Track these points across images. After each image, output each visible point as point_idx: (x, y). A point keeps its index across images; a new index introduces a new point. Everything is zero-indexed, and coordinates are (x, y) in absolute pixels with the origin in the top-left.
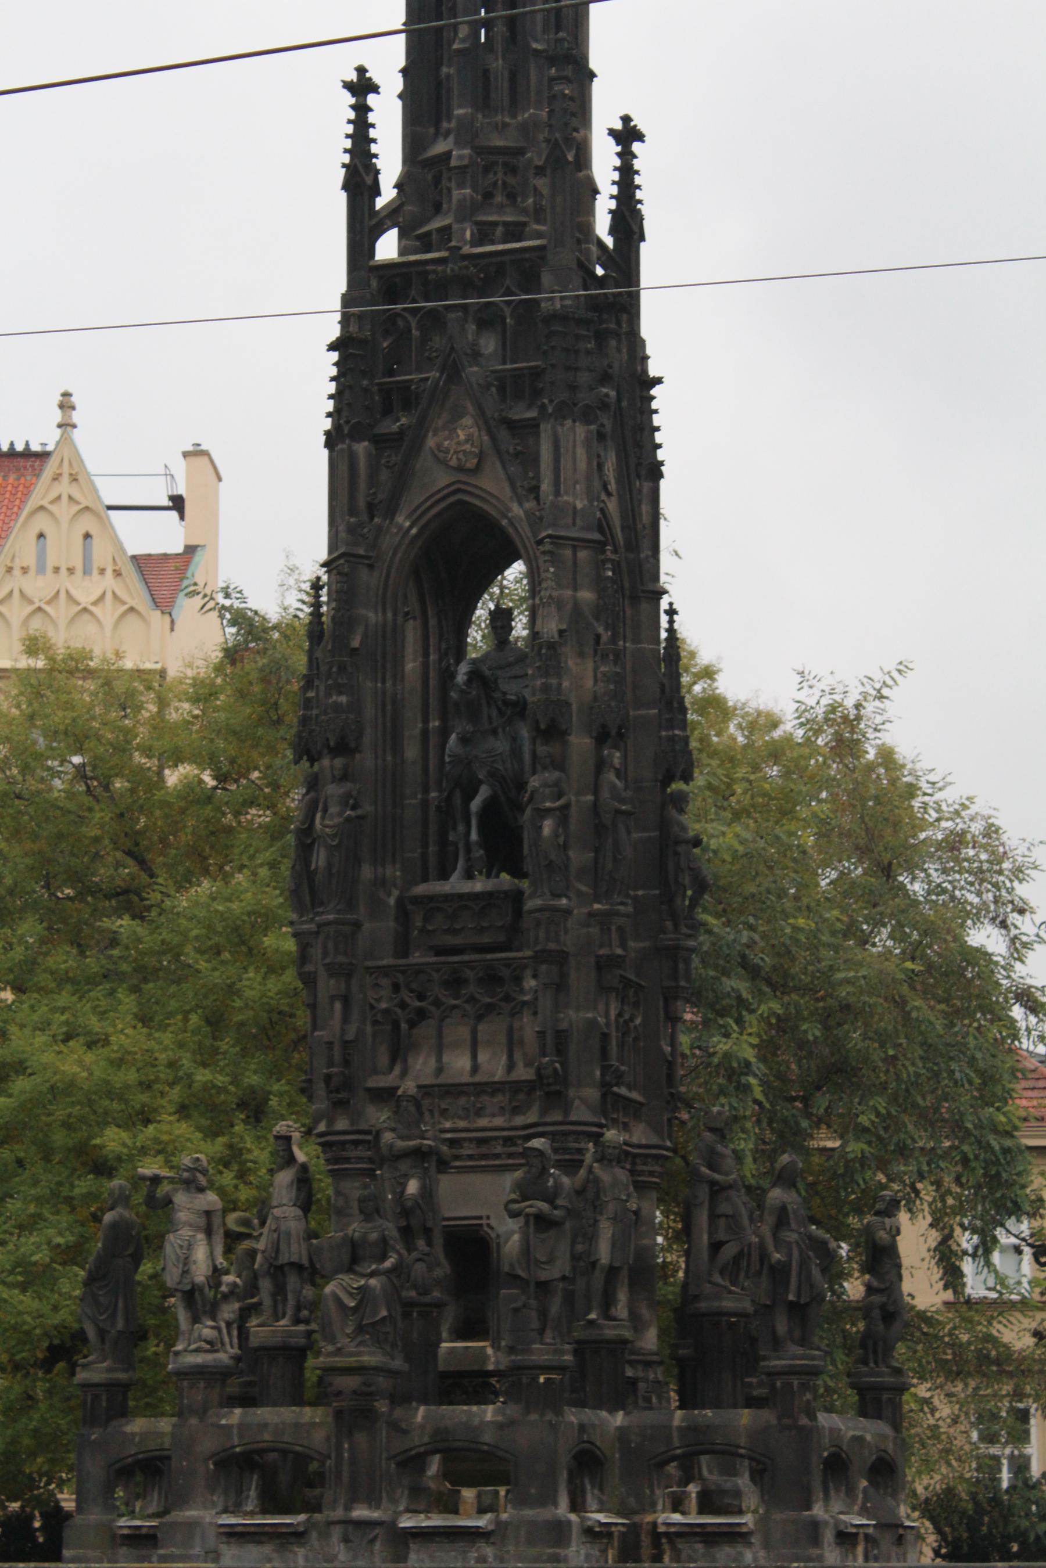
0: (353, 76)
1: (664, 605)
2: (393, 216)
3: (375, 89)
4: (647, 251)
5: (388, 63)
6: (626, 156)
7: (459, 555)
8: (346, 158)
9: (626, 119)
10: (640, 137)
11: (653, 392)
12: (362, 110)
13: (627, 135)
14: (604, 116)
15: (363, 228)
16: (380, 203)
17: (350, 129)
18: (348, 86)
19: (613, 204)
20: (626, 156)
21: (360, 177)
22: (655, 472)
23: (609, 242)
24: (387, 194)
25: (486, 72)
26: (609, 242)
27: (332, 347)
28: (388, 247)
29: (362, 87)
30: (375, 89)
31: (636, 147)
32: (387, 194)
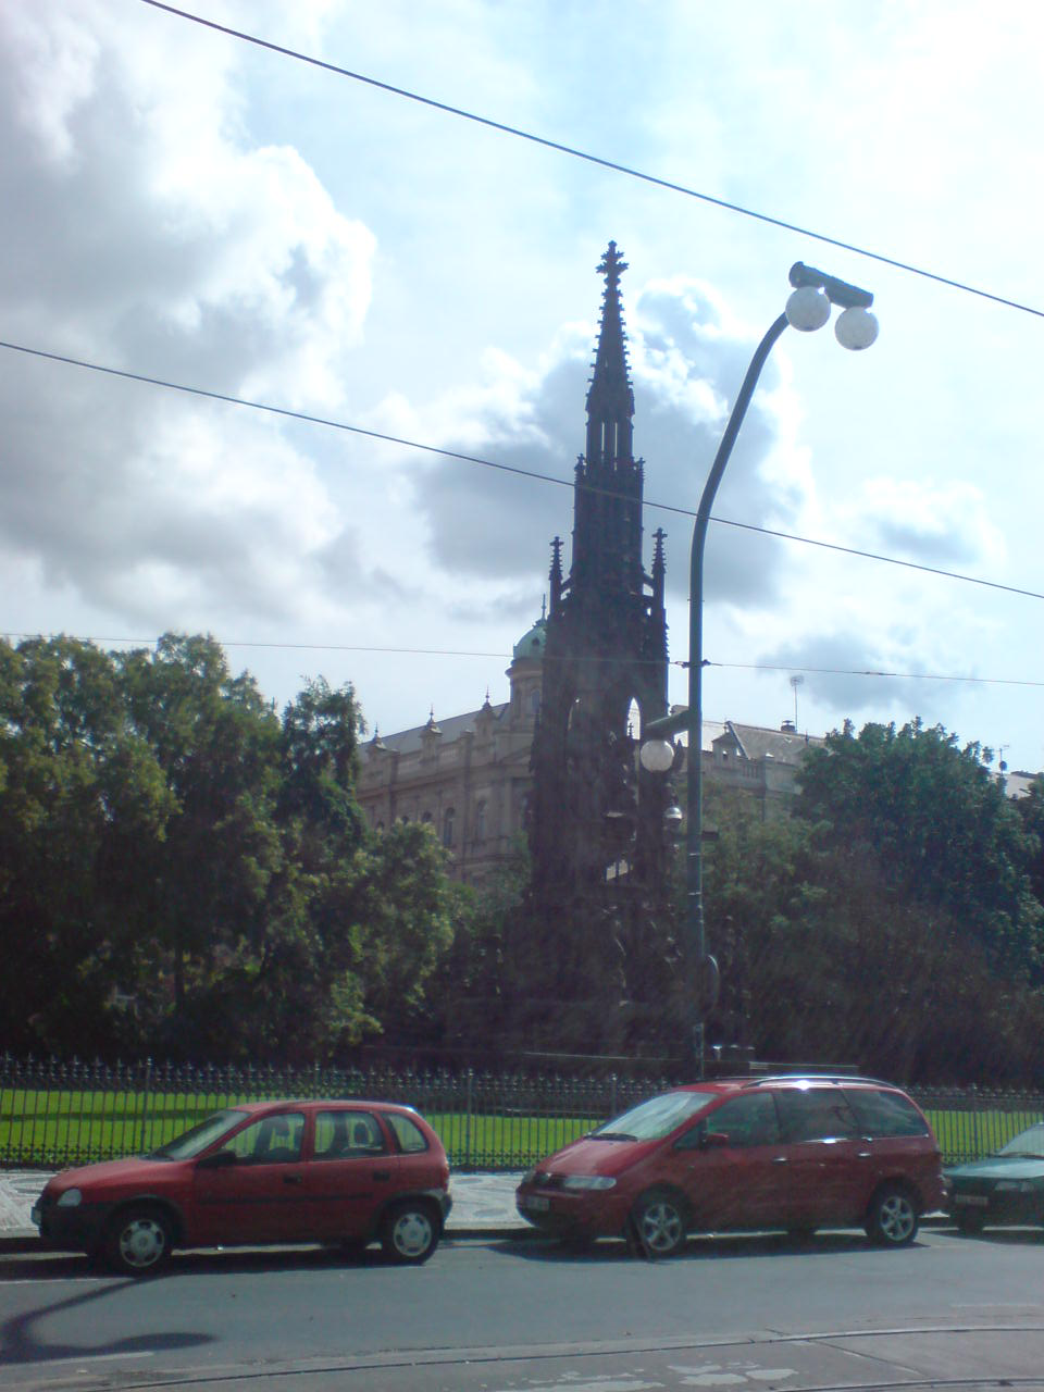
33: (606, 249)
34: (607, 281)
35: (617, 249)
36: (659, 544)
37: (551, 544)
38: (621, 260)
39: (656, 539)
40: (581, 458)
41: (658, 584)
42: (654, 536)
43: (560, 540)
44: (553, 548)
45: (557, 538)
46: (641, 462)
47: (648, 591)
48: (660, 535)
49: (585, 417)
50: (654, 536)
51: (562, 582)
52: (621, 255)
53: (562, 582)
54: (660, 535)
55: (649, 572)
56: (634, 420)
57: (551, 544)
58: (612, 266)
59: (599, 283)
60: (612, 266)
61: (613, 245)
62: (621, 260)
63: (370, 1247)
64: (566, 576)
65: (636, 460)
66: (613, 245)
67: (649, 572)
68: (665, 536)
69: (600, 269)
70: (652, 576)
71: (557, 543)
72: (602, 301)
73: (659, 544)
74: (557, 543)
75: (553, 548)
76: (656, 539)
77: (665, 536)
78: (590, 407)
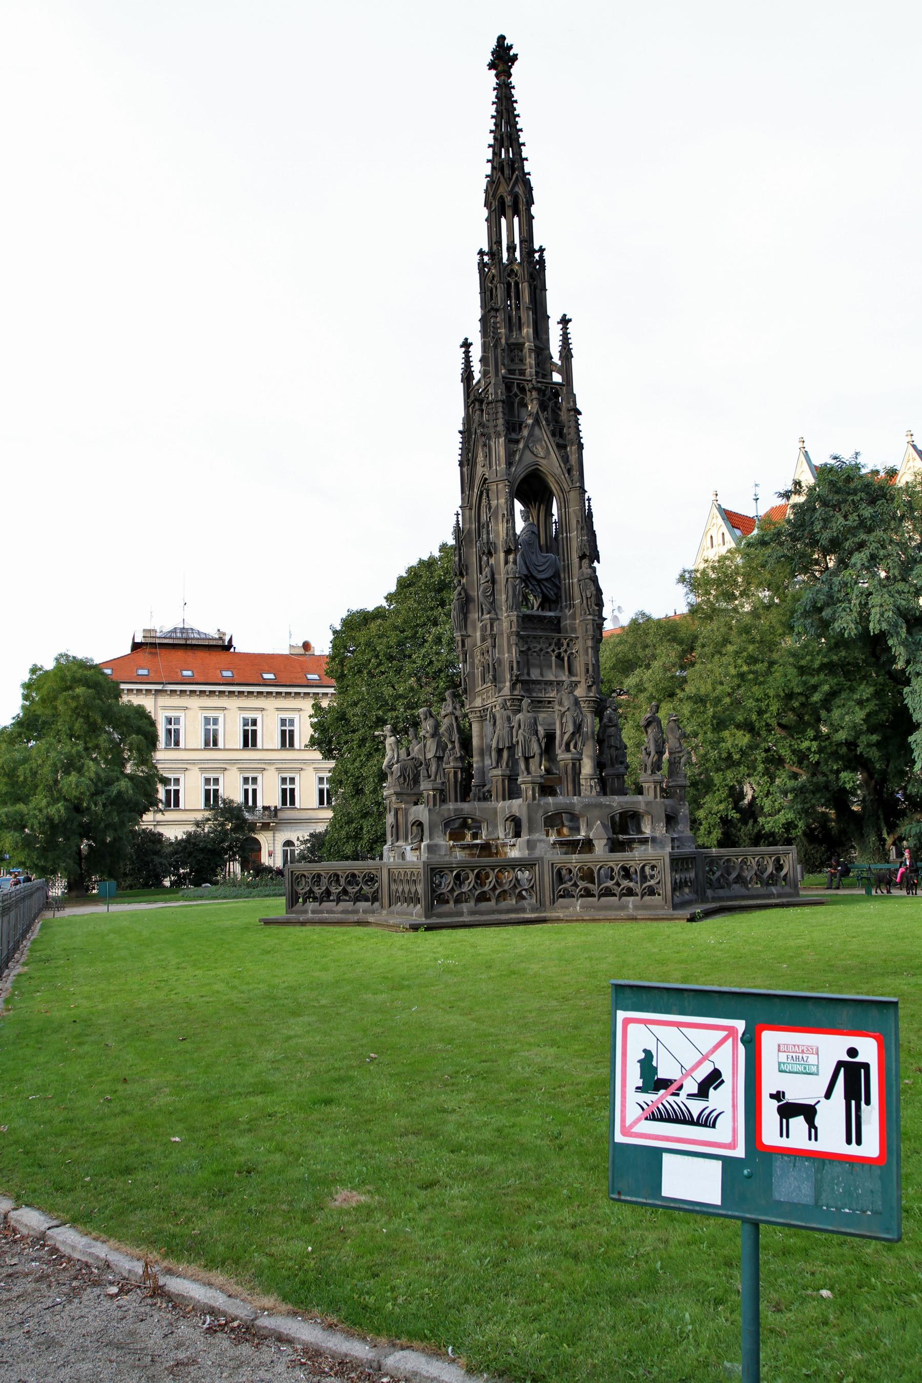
33: (493, 44)
34: (497, 76)
35: (508, 42)
36: (565, 328)
37: (461, 346)
38: (511, 53)
39: (561, 326)
40: (481, 253)
41: (566, 370)
42: (558, 323)
43: (469, 341)
44: (463, 349)
45: (466, 339)
46: (542, 250)
47: (557, 378)
48: (565, 321)
49: (485, 213)
50: (558, 323)
51: (475, 382)
52: (510, 47)
53: (475, 382)
54: (565, 321)
55: (556, 359)
56: (534, 210)
57: (461, 346)
58: (503, 58)
59: (490, 79)
60: (503, 58)
61: (502, 38)
62: (511, 53)
63: (173, 1139)
64: (477, 376)
65: (536, 247)
66: (502, 38)
67: (556, 359)
68: (570, 320)
69: (492, 66)
70: (559, 363)
71: (466, 345)
73: (565, 328)
74: (466, 345)
75: (463, 349)
76: (561, 326)
77: (570, 320)
78: (487, 204)
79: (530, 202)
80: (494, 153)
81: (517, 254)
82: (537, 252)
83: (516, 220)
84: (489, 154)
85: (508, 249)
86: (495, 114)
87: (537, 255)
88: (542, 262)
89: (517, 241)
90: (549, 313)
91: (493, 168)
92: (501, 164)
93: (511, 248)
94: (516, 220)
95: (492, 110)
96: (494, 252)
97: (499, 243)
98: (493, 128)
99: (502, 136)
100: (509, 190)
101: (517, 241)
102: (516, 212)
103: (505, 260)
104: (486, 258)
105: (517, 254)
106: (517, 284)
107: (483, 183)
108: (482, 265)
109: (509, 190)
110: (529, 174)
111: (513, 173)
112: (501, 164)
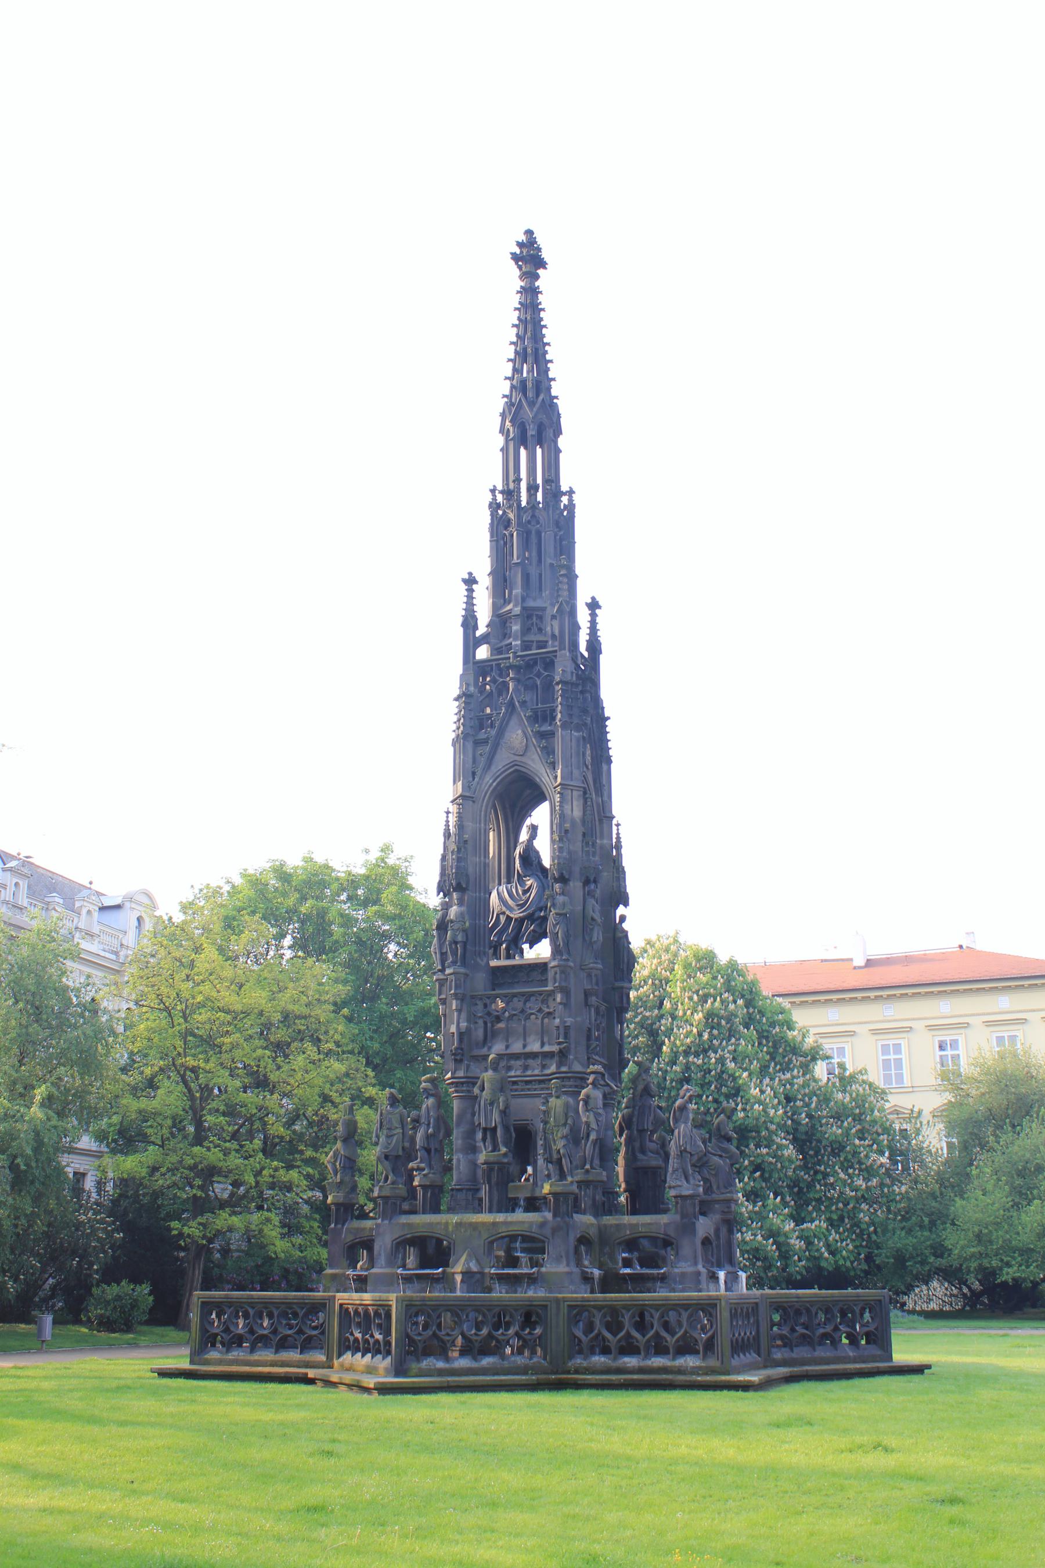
0: (467, 577)
1: (614, 822)
2: (485, 639)
3: (476, 582)
4: (603, 659)
5: (483, 568)
6: (593, 616)
7: (517, 796)
8: (463, 613)
9: (593, 598)
10: (599, 607)
11: (607, 723)
12: (470, 591)
13: (593, 606)
14: (582, 598)
15: (471, 643)
16: (478, 634)
17: (465, 599)
18: (465, 581)
19: (588, 638)
20: (593, 616)
21: (469, 622)
22: (609, 761)
23: (586, 654)
24: (482, 630)
25: (528, 575)
26: (586, 654)
27: (456, 699)
28: (482, 653)
29: (470, 581)
30: (476, 582)
31: (598, 611)
32: (482, 630)
49: (500, 441)
58: (529, 258)
59: (512, 278)
60: (529, 258)
61: (529, 233)
66: (529, 233)
72: (515, 300)
79: (558, 431)
80: (515, 370)
81: (540, 497)
82: (565, 494)
83: (539, 451)
84: (508, 369)
85: (529, 489)
86: (517, 322)
87: (565, 500)
88: (571, 507)
89: (539, 481)
90: (577, 572)
91: (512, 387)
92: (523, 383)
93: (532, 488)
94: (539, 451)
95: (514, 317)
96: (511, 493)
97: (518, 480)
98: (515, 339)
99: (525, 349)
100: (532, 417)
101: (539, 481)
102: (540, 443)
103: (524, 504)
104: (500, 498)
105: (540, 497)
106: (539, 534)
107: (500, 404)
108: (494, 506)
109: (532, 417)
110: (556, 397)
111: (538, 396)
112: (523, 383)
